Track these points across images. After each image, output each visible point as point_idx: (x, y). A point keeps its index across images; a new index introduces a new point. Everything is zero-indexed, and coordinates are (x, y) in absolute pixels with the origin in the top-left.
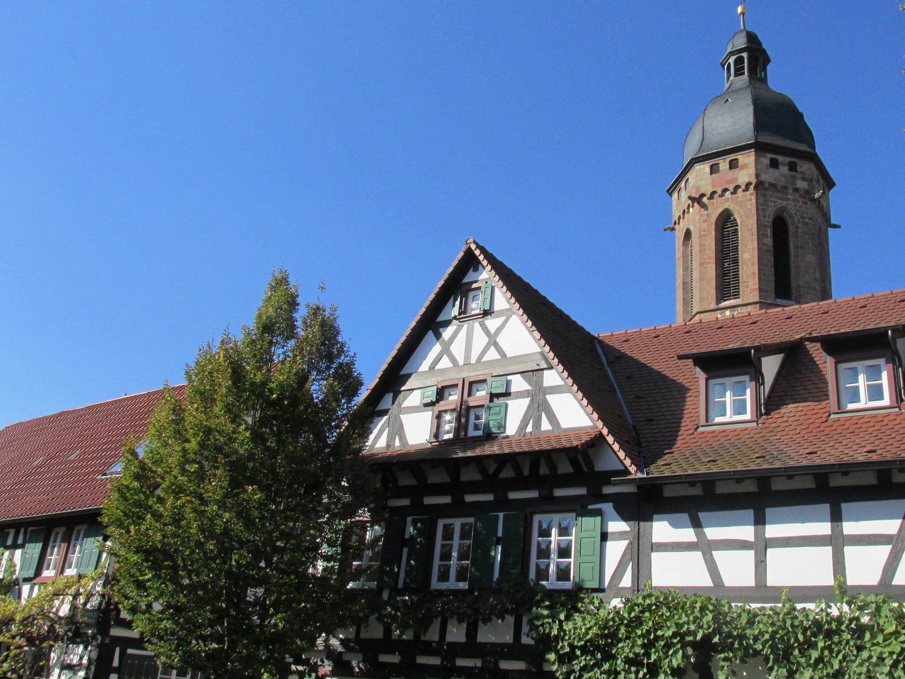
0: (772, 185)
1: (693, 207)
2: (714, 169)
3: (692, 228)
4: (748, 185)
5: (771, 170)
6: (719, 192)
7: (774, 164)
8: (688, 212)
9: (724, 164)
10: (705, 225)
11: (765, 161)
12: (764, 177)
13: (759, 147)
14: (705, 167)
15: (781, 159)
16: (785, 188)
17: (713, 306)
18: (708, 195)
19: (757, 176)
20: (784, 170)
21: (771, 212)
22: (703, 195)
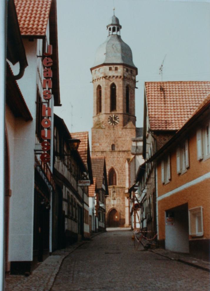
0: (127, 77)
1: (102, 79)
2: (110, 69)
3: (101, 85)
4: (121, 77)
5: (126, 73)
6: (112, 77)
7: (127, 71)
8: (100, 80)
9: (113, 67)
10: (106, 86)
11: (125, 69)
12: (125, 75)
13: (123, 65)
14: (107, 67)
15: (129, 69)
16: (129, 78)
17: (109, 112)
18: (108, 77)
19: (123, 74)
20: (129, 73)
21: (125, 86)
22: (106, 76)
